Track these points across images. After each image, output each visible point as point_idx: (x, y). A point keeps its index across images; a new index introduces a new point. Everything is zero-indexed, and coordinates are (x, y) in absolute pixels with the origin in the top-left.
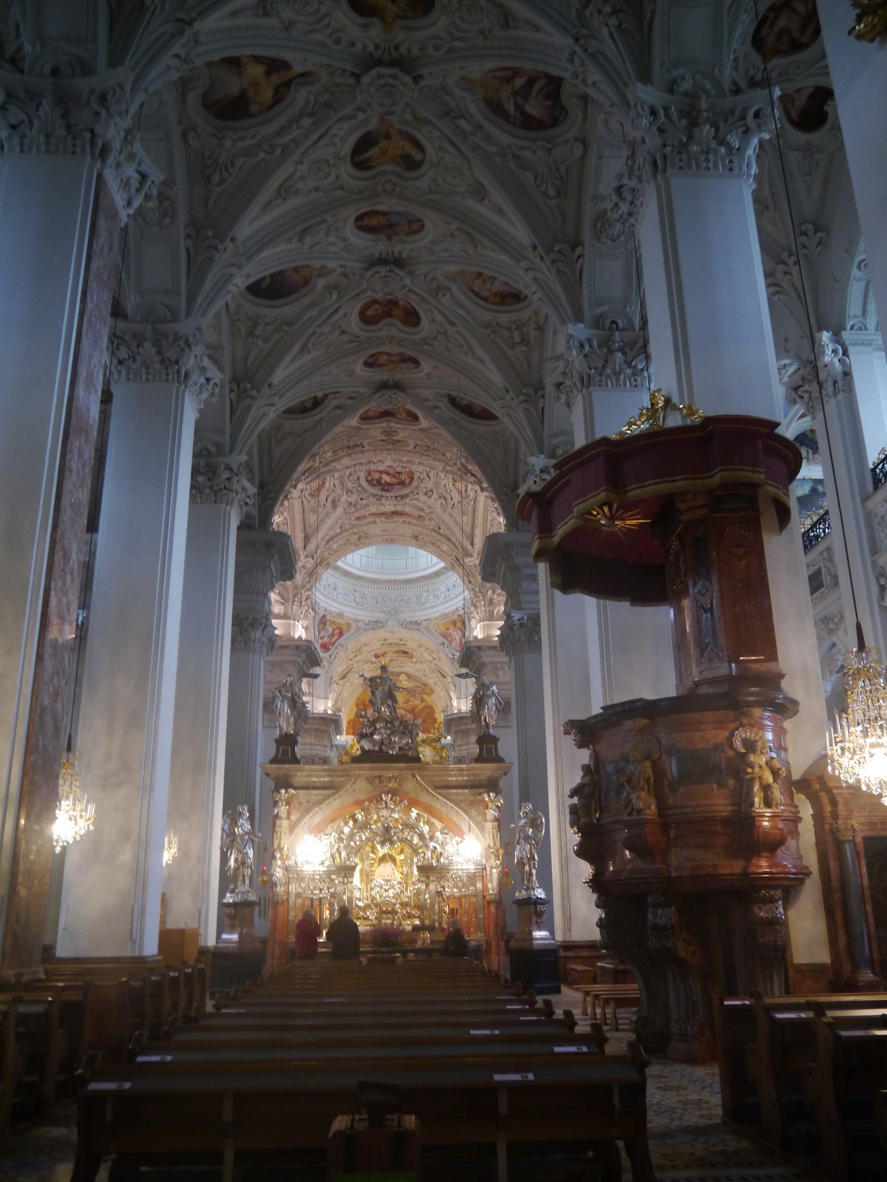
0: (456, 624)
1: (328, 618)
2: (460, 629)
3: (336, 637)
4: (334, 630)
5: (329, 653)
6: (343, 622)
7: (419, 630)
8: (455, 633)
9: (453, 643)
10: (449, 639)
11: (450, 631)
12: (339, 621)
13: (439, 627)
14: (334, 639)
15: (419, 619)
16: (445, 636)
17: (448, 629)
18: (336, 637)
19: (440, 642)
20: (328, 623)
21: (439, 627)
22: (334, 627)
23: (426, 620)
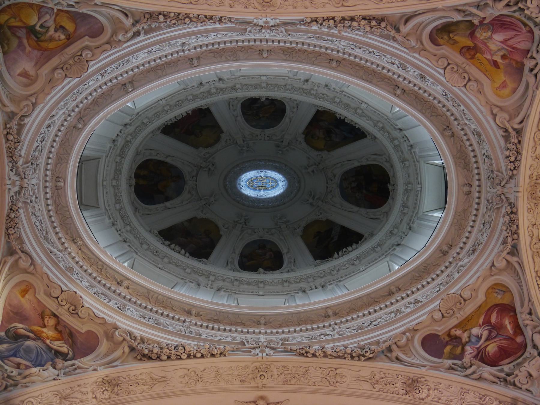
0: (469, 48)
1: (440, 329)
2: (472, 35)
3: (507, 322)
4: (487, 322)
5: (529, 348)
6: (481, 297)
7: (519, 132)
8: (493, 47)
9: (523, 46)
10: (517, 57)
11: (498, 58)
12: (469, 309)
13: (504, 85)
14: (509, 327)
15: (500, 133)
16: (519, 69)
17: (495, 64)
18: (507, 322)
19: (532, 80)
20: (458, 332)
21: (504, 85)
22: (481, 321)
23: (494, 116)
